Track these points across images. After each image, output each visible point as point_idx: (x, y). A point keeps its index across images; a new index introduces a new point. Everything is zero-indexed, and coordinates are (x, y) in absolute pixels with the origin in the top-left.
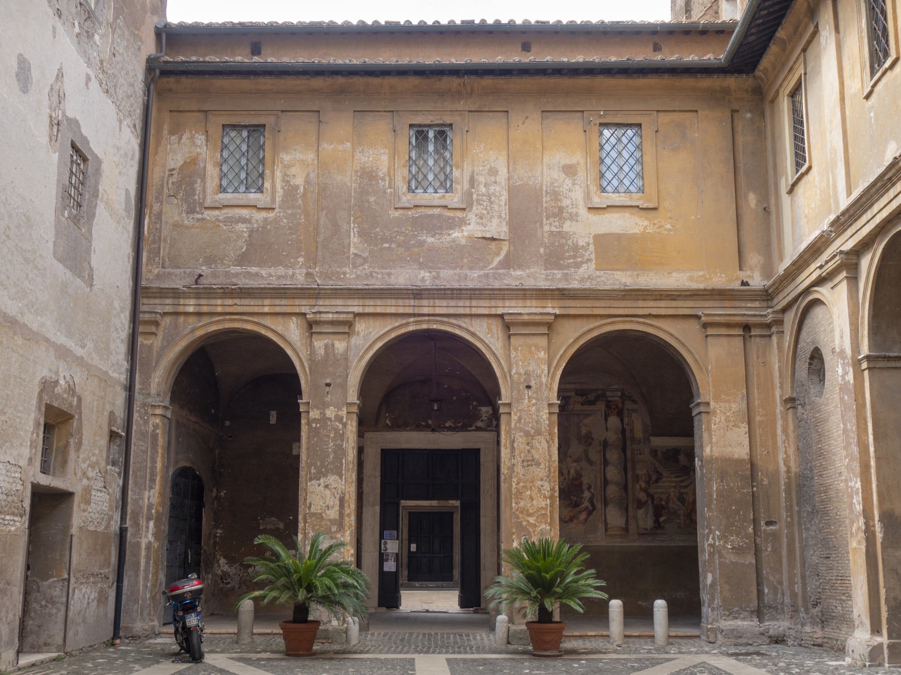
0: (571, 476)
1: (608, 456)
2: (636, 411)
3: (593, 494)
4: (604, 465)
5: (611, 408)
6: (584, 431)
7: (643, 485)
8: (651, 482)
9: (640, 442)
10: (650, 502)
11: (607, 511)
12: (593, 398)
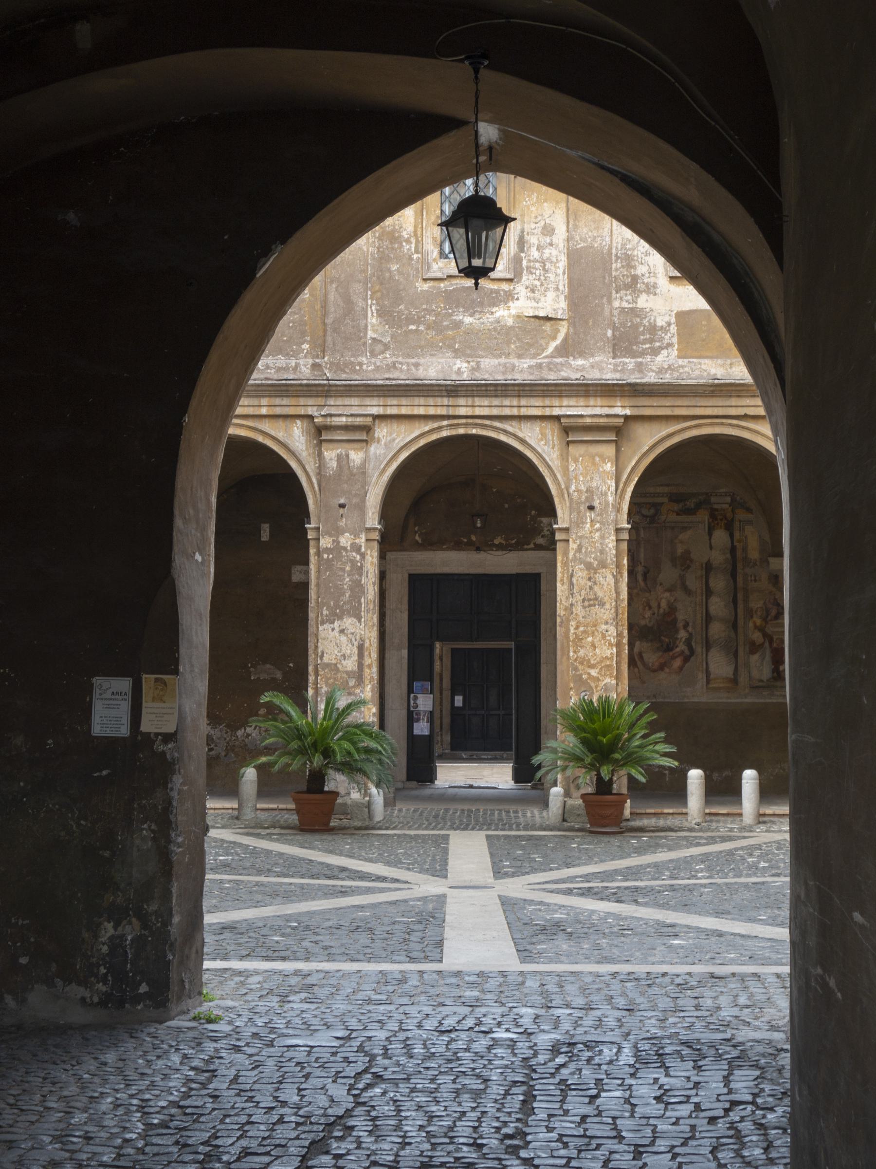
0: (661, 611)
1: (712, 584)
2: (750, 522)
3: (691, 634)
6: (680, 551)
7: (759, 622)
8: (769, 618)
9: (755, 564)
10: (767, 644)
12: (693, 506)
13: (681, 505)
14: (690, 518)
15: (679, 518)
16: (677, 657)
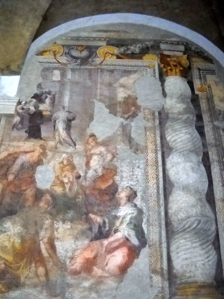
0: (91, 173)
3: (140, 212)
5: (169, 65)
6: (121, 95)
11: (173, 248)
13: (122, 50)
16: (117, 248)
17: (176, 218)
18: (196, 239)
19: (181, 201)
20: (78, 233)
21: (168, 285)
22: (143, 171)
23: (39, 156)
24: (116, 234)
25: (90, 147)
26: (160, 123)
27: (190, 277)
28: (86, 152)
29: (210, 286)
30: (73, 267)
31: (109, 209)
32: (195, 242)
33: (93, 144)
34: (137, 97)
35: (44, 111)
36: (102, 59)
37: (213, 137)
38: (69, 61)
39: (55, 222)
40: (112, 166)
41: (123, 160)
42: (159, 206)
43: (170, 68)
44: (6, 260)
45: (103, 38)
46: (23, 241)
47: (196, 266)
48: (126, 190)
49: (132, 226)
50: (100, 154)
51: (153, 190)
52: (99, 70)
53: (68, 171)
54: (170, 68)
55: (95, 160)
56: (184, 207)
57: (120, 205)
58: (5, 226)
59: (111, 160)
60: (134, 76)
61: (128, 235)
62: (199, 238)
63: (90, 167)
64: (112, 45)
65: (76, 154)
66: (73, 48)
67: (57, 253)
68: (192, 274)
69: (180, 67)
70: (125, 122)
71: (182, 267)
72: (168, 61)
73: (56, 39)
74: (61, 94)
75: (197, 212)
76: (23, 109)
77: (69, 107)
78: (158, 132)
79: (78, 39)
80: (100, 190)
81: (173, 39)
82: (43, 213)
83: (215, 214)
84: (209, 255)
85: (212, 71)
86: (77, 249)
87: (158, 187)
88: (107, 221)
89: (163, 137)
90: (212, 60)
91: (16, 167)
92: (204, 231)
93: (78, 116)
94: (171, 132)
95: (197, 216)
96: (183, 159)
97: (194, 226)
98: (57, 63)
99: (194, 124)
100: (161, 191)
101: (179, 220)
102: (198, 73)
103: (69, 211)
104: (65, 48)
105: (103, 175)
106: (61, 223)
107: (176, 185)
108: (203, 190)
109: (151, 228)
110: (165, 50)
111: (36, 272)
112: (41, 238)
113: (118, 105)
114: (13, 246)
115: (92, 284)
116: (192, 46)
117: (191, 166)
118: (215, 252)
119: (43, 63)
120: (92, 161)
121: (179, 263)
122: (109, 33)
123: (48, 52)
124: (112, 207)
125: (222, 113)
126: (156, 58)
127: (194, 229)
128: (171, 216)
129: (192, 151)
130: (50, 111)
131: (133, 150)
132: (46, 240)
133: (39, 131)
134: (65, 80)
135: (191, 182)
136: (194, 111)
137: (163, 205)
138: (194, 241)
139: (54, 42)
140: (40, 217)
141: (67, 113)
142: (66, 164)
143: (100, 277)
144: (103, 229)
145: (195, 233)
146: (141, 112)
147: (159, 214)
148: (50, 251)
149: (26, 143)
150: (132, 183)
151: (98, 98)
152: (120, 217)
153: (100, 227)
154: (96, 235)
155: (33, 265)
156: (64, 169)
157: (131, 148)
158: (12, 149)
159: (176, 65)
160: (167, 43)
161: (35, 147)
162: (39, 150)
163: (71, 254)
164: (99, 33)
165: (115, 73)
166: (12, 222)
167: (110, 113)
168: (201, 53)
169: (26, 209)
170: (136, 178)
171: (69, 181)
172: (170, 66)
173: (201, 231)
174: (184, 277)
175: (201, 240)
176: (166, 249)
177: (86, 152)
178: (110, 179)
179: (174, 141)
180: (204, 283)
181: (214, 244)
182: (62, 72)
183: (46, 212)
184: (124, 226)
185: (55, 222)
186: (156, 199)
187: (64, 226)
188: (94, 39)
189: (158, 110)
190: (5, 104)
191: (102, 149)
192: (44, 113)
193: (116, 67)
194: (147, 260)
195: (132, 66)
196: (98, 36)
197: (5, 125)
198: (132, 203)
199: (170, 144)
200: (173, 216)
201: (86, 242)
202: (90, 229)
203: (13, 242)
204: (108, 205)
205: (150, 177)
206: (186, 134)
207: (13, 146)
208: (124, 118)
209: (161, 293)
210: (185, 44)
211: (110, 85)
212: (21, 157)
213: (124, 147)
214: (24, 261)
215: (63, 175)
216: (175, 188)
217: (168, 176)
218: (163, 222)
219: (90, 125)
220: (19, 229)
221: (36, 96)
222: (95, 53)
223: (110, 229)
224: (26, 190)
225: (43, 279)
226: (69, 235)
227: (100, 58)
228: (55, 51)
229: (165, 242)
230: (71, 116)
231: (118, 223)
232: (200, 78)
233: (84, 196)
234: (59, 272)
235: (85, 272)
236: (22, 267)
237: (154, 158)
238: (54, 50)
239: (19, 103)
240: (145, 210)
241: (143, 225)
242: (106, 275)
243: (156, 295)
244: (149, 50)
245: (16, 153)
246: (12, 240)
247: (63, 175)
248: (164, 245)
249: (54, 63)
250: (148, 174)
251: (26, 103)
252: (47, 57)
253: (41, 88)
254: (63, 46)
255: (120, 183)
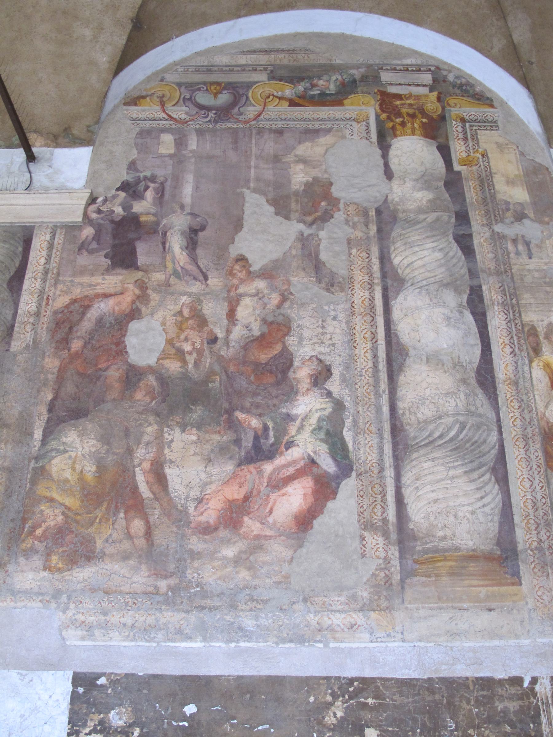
0: (238, 332)
3: (339, 406)
4: (385, 290)
5: (399, 114)
11: (407, 478)
13: (301, 88)
14: (324, 112)
15: (297, 112)
17: (413, 418)
18: (457, 461)
19: (424, 385)
20: (212, 451)
21: (397, 554)
22: (344, 325)
23: (133, 302)
24: (290, 451)
25: (235, 281)
26: (380, 230)
27: (444, 538)
28: (229, 291)
29: (489, 557)
30: (203, 519)
31: (275, 401)
32: (454, 467)
33: (242, 275)
34: (332, 180)
35: (142, 214)
36: (259, 108)
37: (491, 255)
38: (191, 116)
39: (166, 429)
40: (281, 318)
41: (303, 305)
42: (378, 395)
43: (401, 119)
44: (66, 507)
45: (261, 65)
46: (101, 468)
47: (456, 516)
48: (310, 363)
49: (322, 435)
50: (257, 294)
51: (365, 364)
52: (254, 131)
53: (192, 328)
54: (401, 119)
55: (246, 306)
56: (430, 396)
57: (297, 393)
58: (64, 439)
59: (279, 306)
60: (325, 140)
61: (315, 452)
62: (463, 458)
63: (237, 320)
64: (281, 80)
65: (208, 297)
66: (199, 89)
67: (170, 490)
68: (449, 533)
69: (422, 118)
70: (307, 231)
71: (427, 517)
72: (397, 106)
73: (165, 70)
74: (177, 180)
75: (457, 405)
76: (99, 211)
77: (193, 205)
78: (375, 251)
79: (209, 70)
80: (257, 364)
81: (409, 61)
82: (141, 413)
83: (496, 409)
84: (484, 494)
85: (491, 122)
86: (211, 483)
87: (375, 356)
88: (270, 424)
89: (384, 259)
90: (492, 100)
91: (87, 324)
92: (473, 444)
93: (210, 222)
94: (402, 248)
95: (457, 414)
96: (428, 301)
97: (452, 433)
98: (167, 120)
99: (451, 231)
100: (382, 366)
101: (419, 422)
102: (460, 129)
103: (193, 408)
104: (183, 89)
105: (263, 336)
106: (177, 431)
107: (412, 352)
108: (470, 363)
109: (361, 438)
110: (391, 84)
111: (127, 528)
112: (136, 462)
113: (293, 199)
114: (81, 478)
115: (241, 552)
116: (450, 71)
117: (444, 314)
118: (497, 486)
119: (140, 120)
120: (239, 309)
121: (420, 509)
122: (273, 56)
123: (148, 98)
124: (281, 397)
125: (511, 207)
126: (373, 102)
127: (451, 440)
128: (404, 414)
129: (447, 285)
130: (155, 215)
131: (323, 285)
132: (146, 465)
133: (133, 253)
134: (184, 152)
135: (445, 346)
136: (451, 205)
137: (387, 392)
138: (452, 465)
139: (159, 79)
140: (136, 420)
141: (189, 217)
142: (187, 316)
143: (257, 537)
144: (262, 441)
145: (454, 449)
146: (339, 210)
147: (378, 410)
148: (155, 487)
149: (107, 277)
150: (323, 350)
151: (252, 185)
152: (297, 416)
153: (256, 438)
154: (247, 453)
155: (122, 515)
156: (184, 326)
157: (319, 281)
158: (79, 290)
159: (415, 113)
160: (395, 69)
161: (126, 285)
162: (133, 290)
163: (198, 493)
164: (254, 56)
165: (287, 135)
166: (79, 432)
167: (277, 214)
168: (468, 88)
169: (107, 406)
170: (331, 339)
171: (194, 348)
172: (400, 117)
173: (468, 445)
174: (431, 538)
175: (466, 464)
176: (393, 481)
177: (229, 291)
178: (277, 343)
179: (408, 265)
180: (474, 550)
181: (494, 470)
182: (177, 137)
183: (147, 411)
184: (306, 434)
185: (166, 429)
186: (371, 380)
187: (184, 436)
188: (243, 68)
189: (376, 205)
190: (62, 202)
191: (261, 284)
192: (143, 219)
193: (289, 122)
194: (353, 502)
195: (321, 120)
196: (250, 63)
197: (64, 244)
198: (320, 388)
199: (400, 271)
200: (408, 415)
201: (229, 467)
202: (237, 442)
203: (82, 471)
204: (273, 394)
205: (359, 338)
206: (434, 251)
207: (81, 284)
208: (305, 223)
209: (382, 569)
210: (432, 69)
211: (276, 159)
212: (96, 306)
213: (306, 280)
214: (104, 509)
215: (182, 337)
216: (411, 359)
217: (396, 335)
218: (387, 427)
219: (237, 239)
220: (93, 446)
221: (125, 187)
222: (245, 97)
223: (278, 441)
224: (106, 369)
225: (141, 542)
226: (195, 454)
227: (254, 106)
228: (163, 96)
229: (390, 466)
230: (195, 224)
231: (293, 429)
232: (465, 139)
233: (224, 377)
234: (175, 529)
235: (226, 527)
236: (98, 521)
237: (367, 300)
238: (160, 94)
239: (93, 200)
240: (348, 402)
241: (345, 433)
242: (268, 532)
243: (373, 575)
244: (356, 87)
245: (87, 296)
246: (78, 468)
247: (182, 337)
248: (389, 473)
249: (161, 120)
250: (354, 331)
251: (105, 200)
252: (147, 108)
253: (137, 170)
254: (179, 85)
255: (298, 351)
